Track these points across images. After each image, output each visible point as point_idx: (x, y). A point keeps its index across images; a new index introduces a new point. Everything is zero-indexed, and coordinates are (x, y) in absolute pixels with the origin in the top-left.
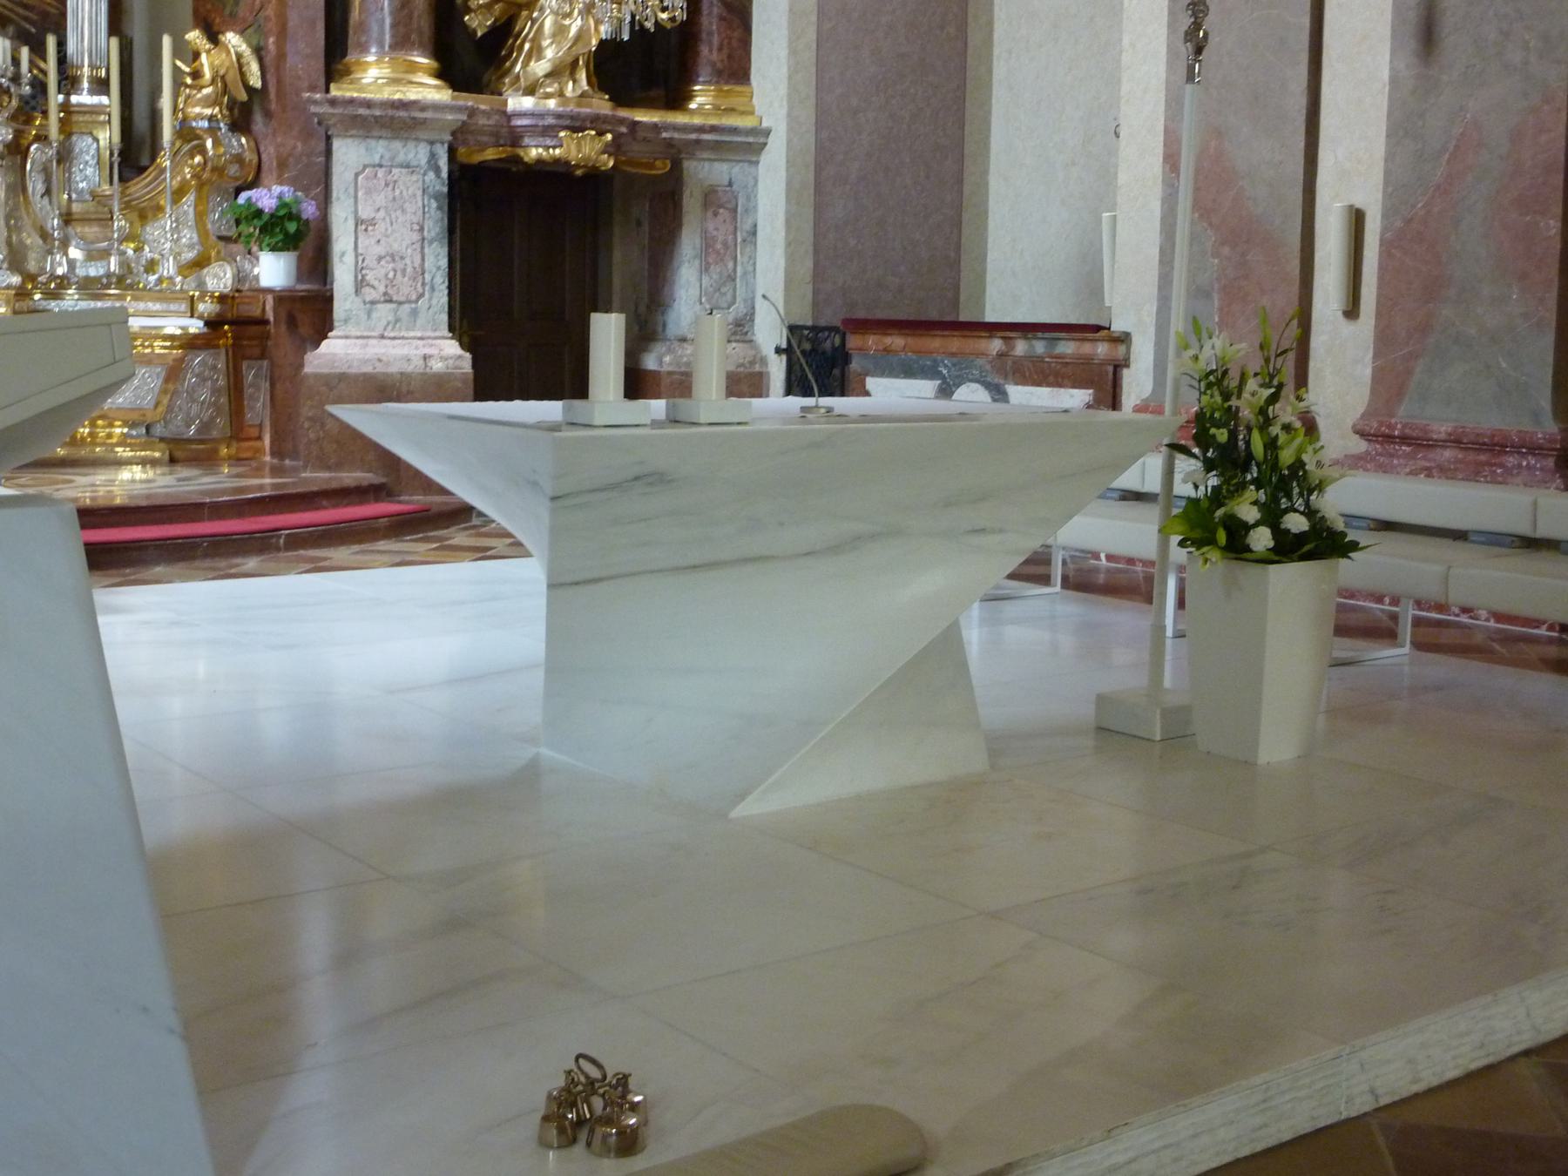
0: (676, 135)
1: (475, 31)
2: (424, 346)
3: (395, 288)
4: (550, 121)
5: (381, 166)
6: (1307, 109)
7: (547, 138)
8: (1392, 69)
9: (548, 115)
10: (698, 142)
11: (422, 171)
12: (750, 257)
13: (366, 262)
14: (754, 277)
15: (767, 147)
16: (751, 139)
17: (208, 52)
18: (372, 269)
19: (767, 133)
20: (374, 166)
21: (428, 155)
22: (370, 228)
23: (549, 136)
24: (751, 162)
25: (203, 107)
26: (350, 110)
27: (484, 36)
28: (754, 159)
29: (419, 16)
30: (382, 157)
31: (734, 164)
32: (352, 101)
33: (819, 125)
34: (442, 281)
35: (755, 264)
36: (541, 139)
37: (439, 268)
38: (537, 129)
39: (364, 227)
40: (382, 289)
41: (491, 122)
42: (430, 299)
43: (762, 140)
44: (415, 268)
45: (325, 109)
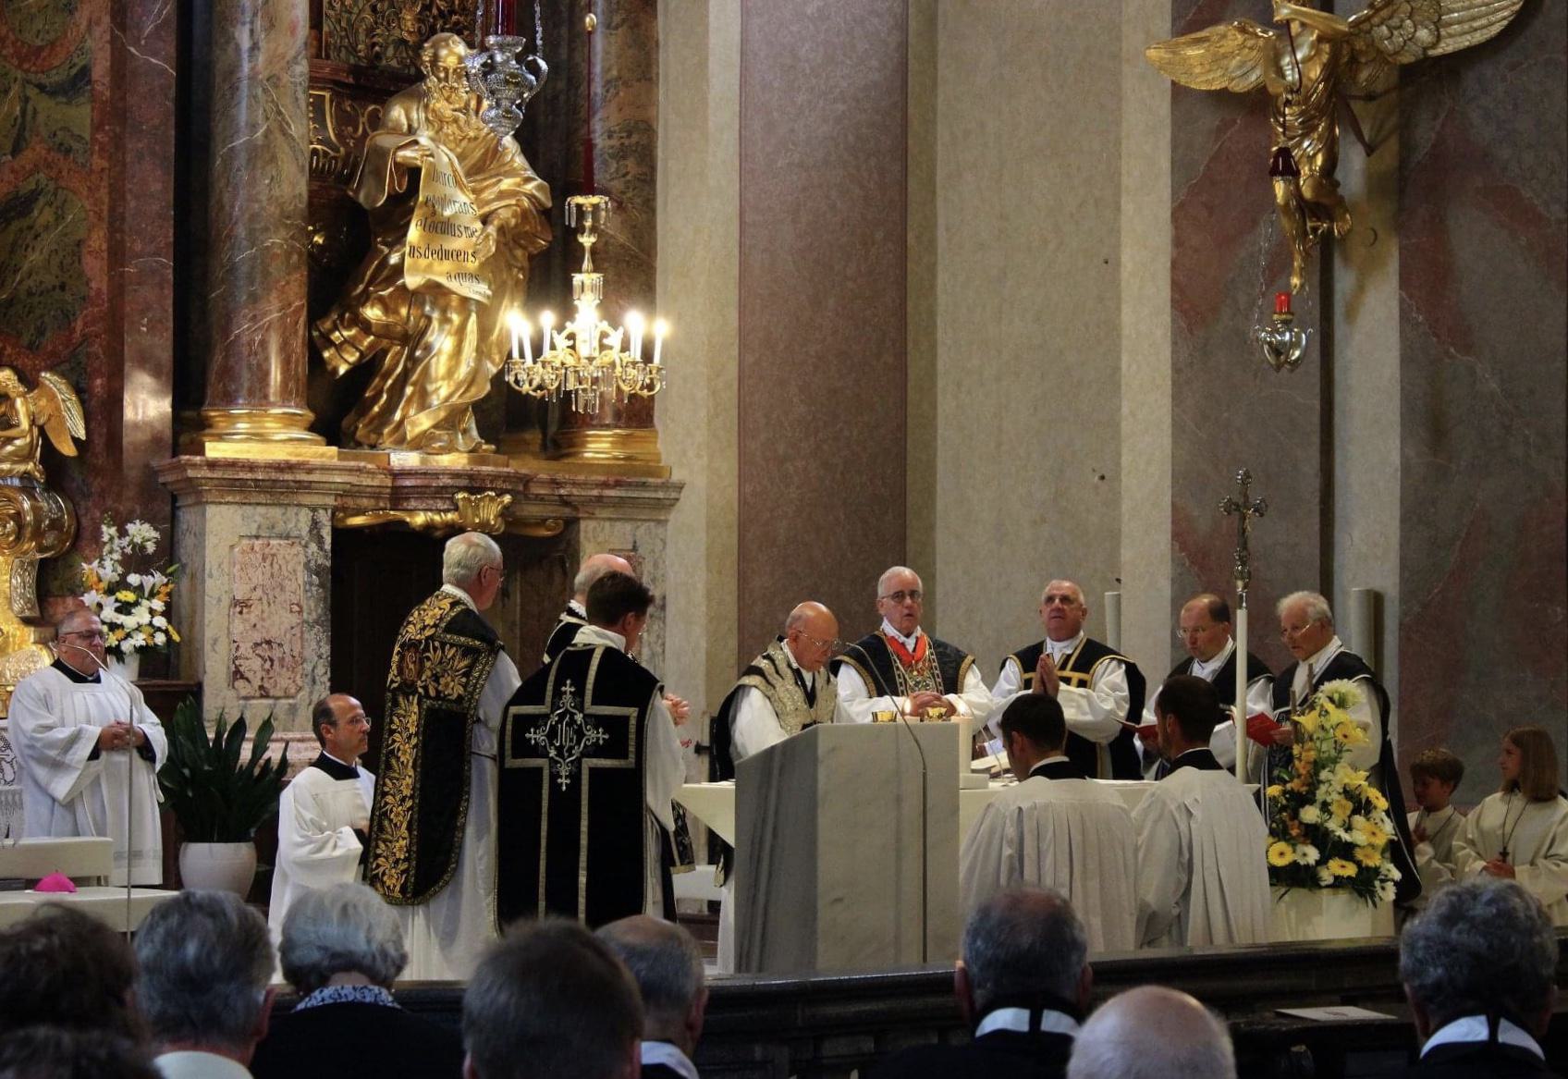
0: (575, 492)
1: (335, 370)
2: (306, 749)
3: (272, 681)
4: (446, 481)
5: (257, 537)
6: (1321, 491)
7: (438, 501)
8: (1403, 455)
9: (443, 474)
10: (600, 498)
11: (303, 542)
12: (658, 636)
13: (242, 650)
14: (664, 661)
15: (679, 504)
16: (661, 495)
17: (23, 395)
18: (247, 659)
19: (680, 487)
20: (250, 537)
21: (310, 524)
22: (245, 610)
23: (441, 498)
24: (659, 522)
25: (14, 462)
26: (229, 475)
27: (347, 373)
28: (663, 518)
29: (297, 360)
30: (259, 527)
31: (639, 523)
32: (233, 464)
33: (742, 478)
34: (323, 671)
35: (663, 644)
36: (431, 502)
37: (320, 657)
38: (428, 491)
39: (238, 609)
40: (257, 683)
41: (376, 483)
42: (311, 693)
43: (674, 495)
44: (293, 657)
45: (205, 473)
